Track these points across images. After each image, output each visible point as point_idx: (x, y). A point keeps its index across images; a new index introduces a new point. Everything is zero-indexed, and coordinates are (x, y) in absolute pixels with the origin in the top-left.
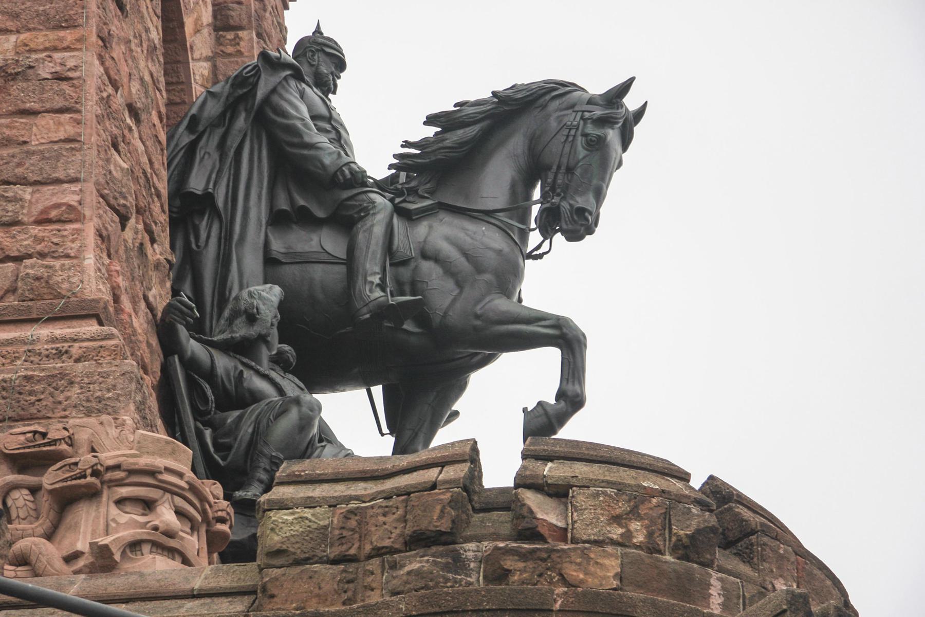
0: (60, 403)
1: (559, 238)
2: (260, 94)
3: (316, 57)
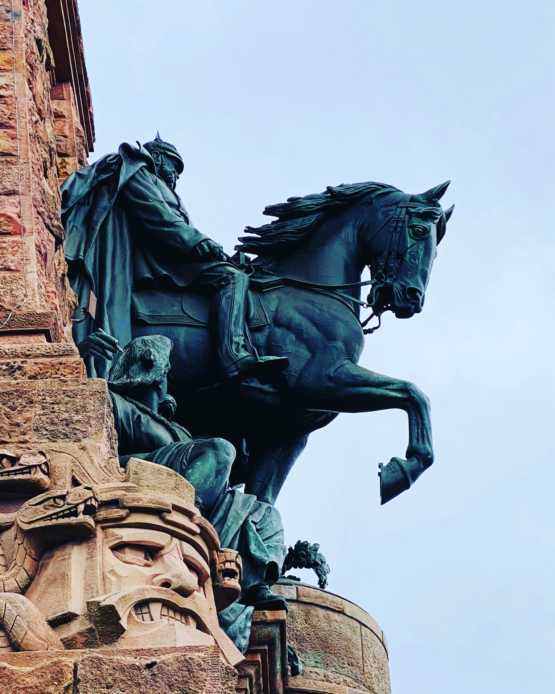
0: (18, 425)
1: (388, 315)
2: (122, 180)
3: (160, 158)
